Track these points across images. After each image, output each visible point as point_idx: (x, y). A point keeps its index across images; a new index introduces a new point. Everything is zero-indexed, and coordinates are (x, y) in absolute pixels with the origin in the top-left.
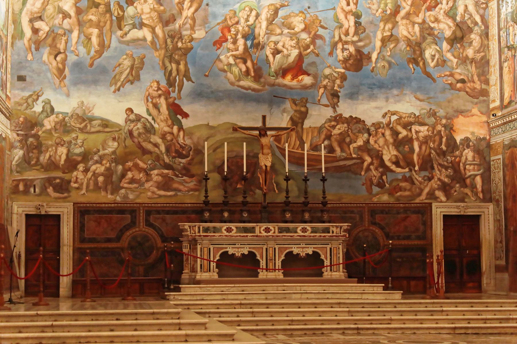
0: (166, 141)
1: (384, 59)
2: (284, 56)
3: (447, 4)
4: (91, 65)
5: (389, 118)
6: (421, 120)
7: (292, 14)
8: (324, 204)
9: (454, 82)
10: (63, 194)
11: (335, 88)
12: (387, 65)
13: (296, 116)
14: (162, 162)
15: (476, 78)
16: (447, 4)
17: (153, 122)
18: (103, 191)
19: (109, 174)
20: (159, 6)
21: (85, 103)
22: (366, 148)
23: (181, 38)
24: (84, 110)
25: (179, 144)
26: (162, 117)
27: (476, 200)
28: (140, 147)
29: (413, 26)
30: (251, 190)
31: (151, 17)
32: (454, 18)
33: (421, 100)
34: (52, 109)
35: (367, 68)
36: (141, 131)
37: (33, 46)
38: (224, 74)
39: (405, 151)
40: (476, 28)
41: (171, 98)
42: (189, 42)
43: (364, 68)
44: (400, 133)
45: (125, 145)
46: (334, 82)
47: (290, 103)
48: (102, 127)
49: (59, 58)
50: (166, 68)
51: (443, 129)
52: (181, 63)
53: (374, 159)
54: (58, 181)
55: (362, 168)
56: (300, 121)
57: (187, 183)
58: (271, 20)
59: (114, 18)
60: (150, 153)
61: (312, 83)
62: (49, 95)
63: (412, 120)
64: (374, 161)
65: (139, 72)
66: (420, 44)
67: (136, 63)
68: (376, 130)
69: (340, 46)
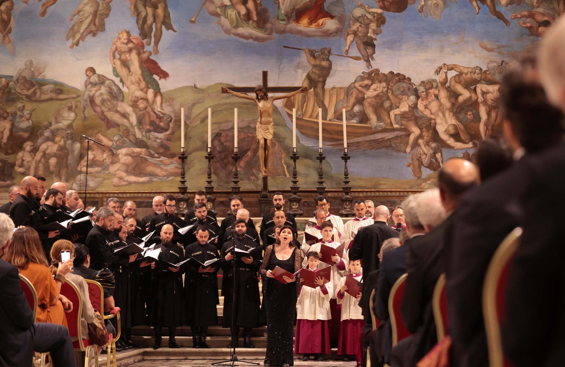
0: (138, 110)
5: (444, 75)
6: (489, 77)
8: (347, 190)
9: (535, 25)
10: (5, 181)
11: (369, 35)
13: (315, 72)
14: (132, 138)
17: (120, 85)
18: (56, 176)
21: (35, 63)
24: (33, 72)
25: (155, 113)
26: (133, 78)
28: (104, 118)
30: (253, 174)
33: (489, 50)
36: (105, 97)
38: (216, 19)
39: (468, 119)
41: (144, 52)
43: (409, 6)
44: (461, 95)
45: (85, 117)
46: (367, 26)
47: (306, 55)
48: (56, 92)
50: (138, 14)
52: (160, 6)
53: (424, 130)
57: (165, 165)
60: (117, 125)
61: (337, 28)
63: (476, 76)
64: (424, 133)
65: (103, 20)
67: (100, 9)
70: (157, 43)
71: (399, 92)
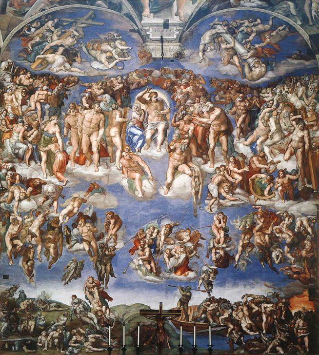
3: (289, 220)
4: (50, 267)
7: (182, 231)
9: (292, 273)
16: (289, 220)
17: (89, 304)
19: (61, 337)
20: (93, 227)
22: (230, 319)
23: (108, 248)
29: (265, 236)
32: (292, 230)
33: (268, 287)
34: (25, 296)
36: (81, 310)
40: (308, 236)
42: (113, 251)
46: (209, 276)
49: (29, 264)
51: (283, 305)
60: (87, 323)
62: (23, 287)
65: (80, 271)
66: (269, 248)
68: (237, 307)
69: (214, 251)
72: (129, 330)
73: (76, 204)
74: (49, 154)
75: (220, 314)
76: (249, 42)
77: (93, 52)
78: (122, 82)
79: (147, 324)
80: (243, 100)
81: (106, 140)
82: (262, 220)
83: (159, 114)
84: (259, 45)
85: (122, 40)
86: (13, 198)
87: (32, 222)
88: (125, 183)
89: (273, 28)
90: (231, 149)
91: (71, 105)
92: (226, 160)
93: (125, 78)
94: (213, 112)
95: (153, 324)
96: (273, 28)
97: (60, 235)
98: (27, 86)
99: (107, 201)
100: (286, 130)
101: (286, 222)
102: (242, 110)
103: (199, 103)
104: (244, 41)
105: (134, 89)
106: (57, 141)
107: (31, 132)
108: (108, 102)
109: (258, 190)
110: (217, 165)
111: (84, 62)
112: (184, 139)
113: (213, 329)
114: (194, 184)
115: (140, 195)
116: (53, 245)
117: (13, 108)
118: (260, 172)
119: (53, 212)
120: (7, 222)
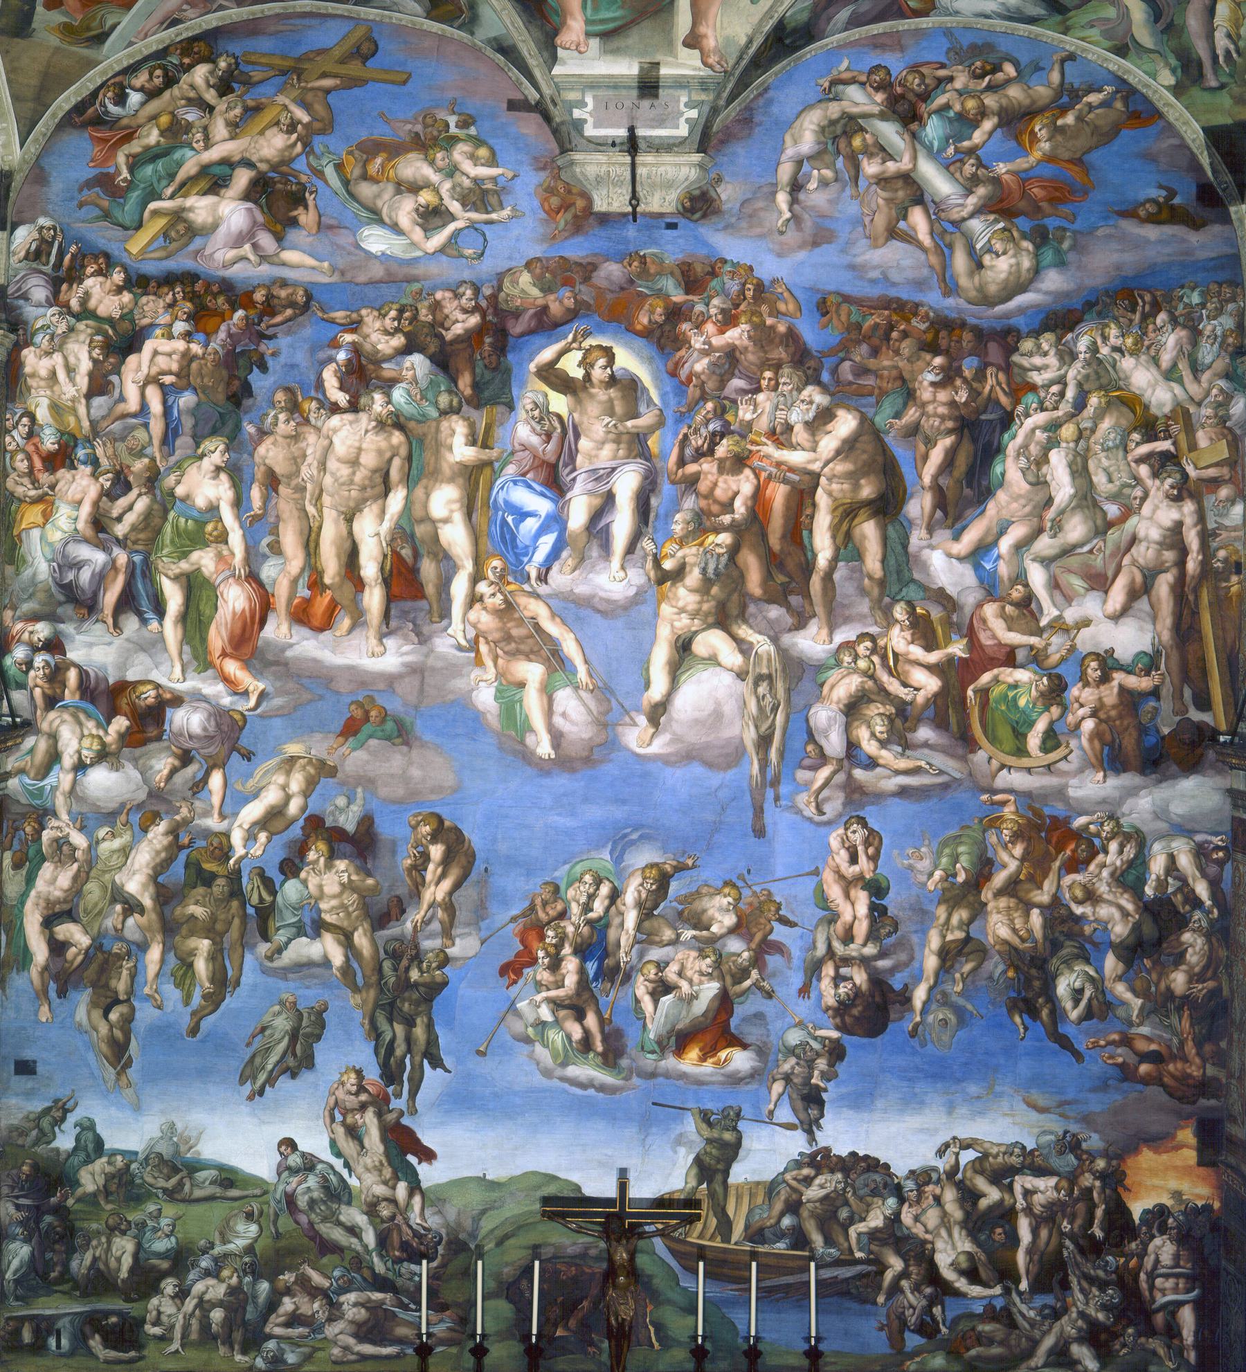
1: (945, 1002)
2: (681, 999)
4: (194, 1031)
6: (1038, 1161)
7: (705, 890)
9: (1132, 1059)
12: (952, 1017)
14: (366, 1273)
15: (1190, 1049)
16: (1121, 852)
17: (345, 1173)
18: (223, 1343)
19: (236, 1300)
20: (363, 875)
22: (893, 1234)
23: (417, 958)
25: (410, 1227)
27: (1178, 1368)
28: (314, 1235)
29: (1027, 915)
30: (592, 1343)
31: (343, 907)
32: (1135, 889)
33: (1041, 1110)
34: (99, 1143)
35: (899, 1027)
36: (316, 1195)
37: (53, 986)
38: (525, 1048)
40: (1197, 915)
43: (891, 1026)
44: (984, 1195)
46: (810, 1065)
48: (221, 1185)
49: (113, 1016)
51: (1098, 1183)
52: (419, 1021)
54: (114, 1319)
55: (880, 1288)
56: (720, 1167)
58: (649, 904)
59: (251, 911)
63: (1015, 1160)
66: (1045, 961)
67: (304, 1023)
69: (829, 970)
70: (413, 1094)
71: (866, 1190)
72: (500, 1274)
73: (296, 782)
74: (194, 585)
75: (852, 1213)
76: (972, 151)
77: (366, 190)
78: (476, 309)
79: (570, 1251)
80: (948, 378)
81: (412, 536)
82: (1018, 850)
83: (620, 434)
84: (1010, 166)
85: (478, 142)
86: (54, 757)
87: (125, 852)
88: (485, 698)
89: (1067, 96)
90: (899, 572)
91: (280, 396)
92: (879, 614)
93: (487, 291)
94: (829, 427)
95: (593, 1252)
96: (1065, 99)
97: (235, 904)
98: (110, 320)
99: (416, 772)
100: (1114, 498)
101: (1109, 860)
102: (943, 418)
103: (775, 389)
104: (951, 150)
105: (522, 335)
106: (223, 538)
107: (123, 502)
108: (424, 384)
109: (1004, 732)
110: (840, 637)
111: (331, 227)
112: (717, 530)
113: (827, 1274)
114: (753, 706)
115: (544, 748)
116: (204, 945)
117: (55, 408)
118: (1009, 658)
119: (207, 813)
120: (31, 852)
